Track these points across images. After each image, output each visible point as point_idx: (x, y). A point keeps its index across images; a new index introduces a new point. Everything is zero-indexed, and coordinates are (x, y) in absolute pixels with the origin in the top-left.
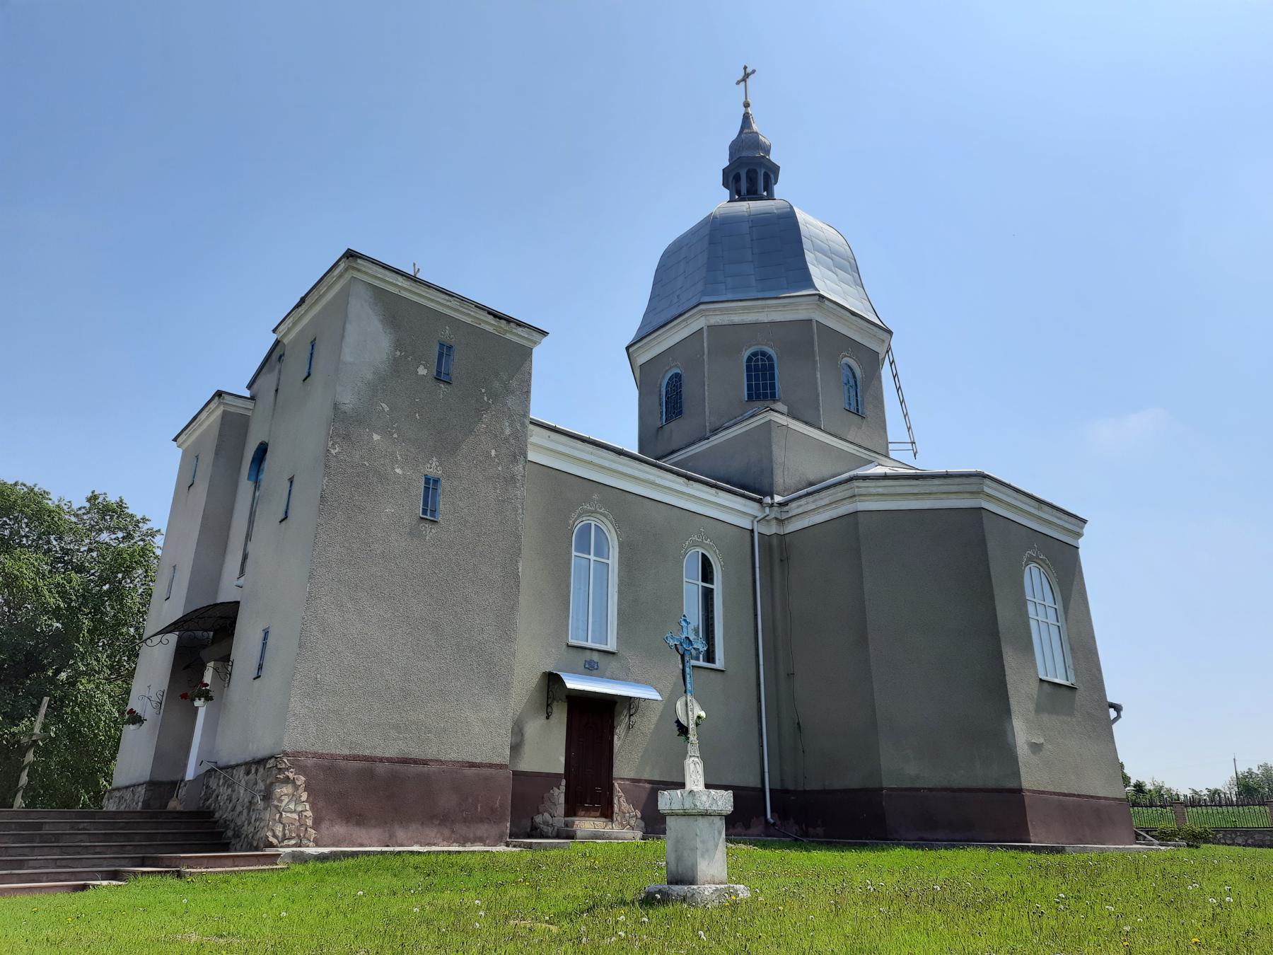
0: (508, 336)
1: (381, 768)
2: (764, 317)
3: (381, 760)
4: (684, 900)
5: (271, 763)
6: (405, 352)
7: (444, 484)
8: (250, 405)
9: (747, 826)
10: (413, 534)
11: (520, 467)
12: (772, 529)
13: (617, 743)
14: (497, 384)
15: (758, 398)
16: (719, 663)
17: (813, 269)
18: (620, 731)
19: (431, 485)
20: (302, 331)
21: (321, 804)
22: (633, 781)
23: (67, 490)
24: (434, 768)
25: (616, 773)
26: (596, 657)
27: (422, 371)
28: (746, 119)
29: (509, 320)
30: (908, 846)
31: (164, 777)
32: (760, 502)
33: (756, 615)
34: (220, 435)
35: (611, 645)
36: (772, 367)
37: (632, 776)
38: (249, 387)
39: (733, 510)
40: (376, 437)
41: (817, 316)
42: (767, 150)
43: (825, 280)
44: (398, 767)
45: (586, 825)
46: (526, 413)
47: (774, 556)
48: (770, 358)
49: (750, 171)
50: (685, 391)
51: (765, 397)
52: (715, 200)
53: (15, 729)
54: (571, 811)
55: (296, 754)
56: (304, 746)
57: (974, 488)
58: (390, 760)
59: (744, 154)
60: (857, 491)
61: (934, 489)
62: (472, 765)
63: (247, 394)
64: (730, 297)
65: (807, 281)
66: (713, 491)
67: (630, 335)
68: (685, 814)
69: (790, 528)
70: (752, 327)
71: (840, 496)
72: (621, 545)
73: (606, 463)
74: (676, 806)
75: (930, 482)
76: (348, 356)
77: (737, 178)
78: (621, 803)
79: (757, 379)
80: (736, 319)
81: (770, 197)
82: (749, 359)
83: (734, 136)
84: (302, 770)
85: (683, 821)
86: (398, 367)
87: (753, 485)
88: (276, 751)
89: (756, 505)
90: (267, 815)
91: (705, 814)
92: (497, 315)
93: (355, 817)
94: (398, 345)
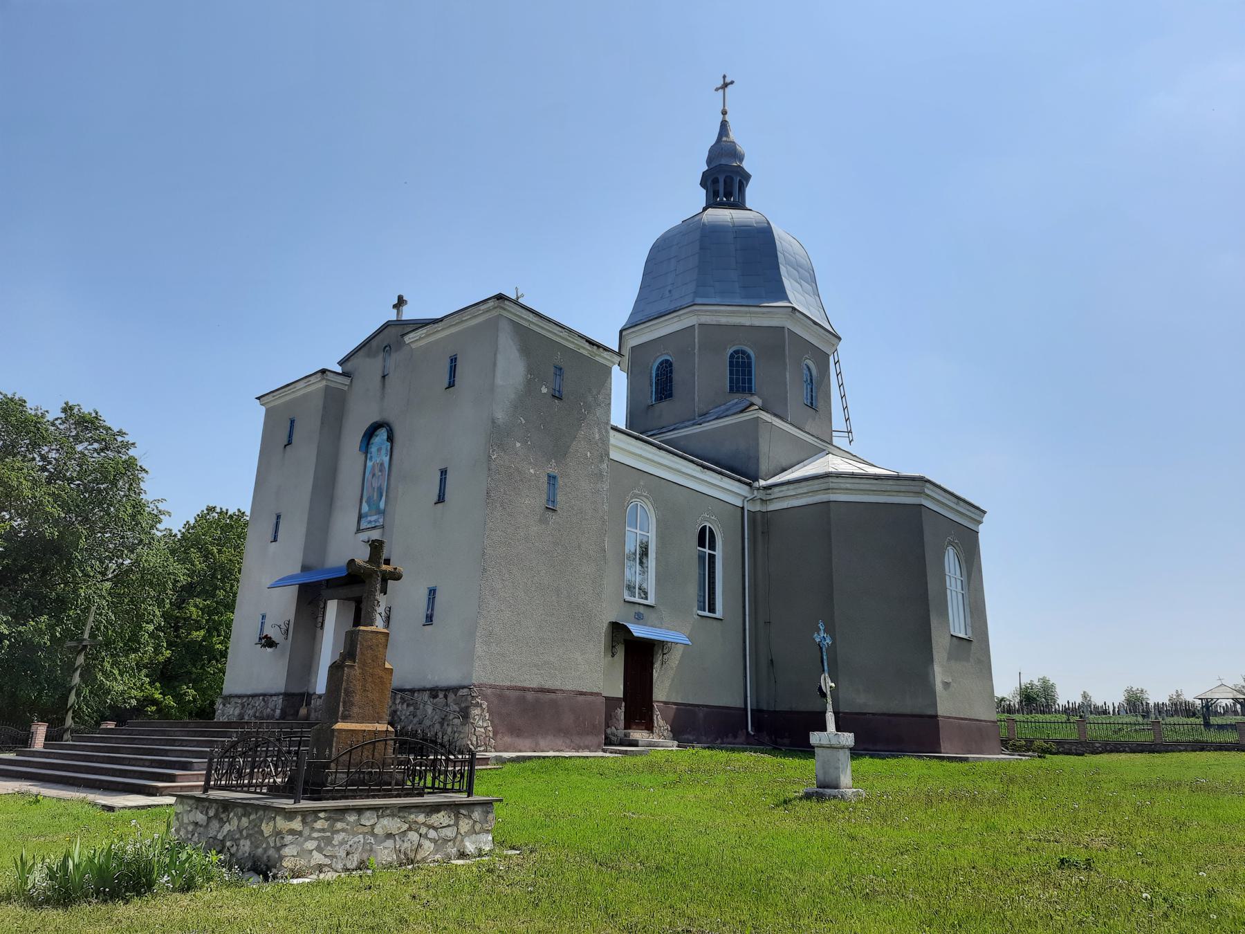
0: (597, 358)
1: (530, 696)
2: (746, 321)
3: (528, 689)
4: (835, 797)
5: (461, 692)
6: (533, 375)
7: (560, 482)
8: (347, 381)
9: (735, 737)
10: (543, 521)
11: (605, 466)
12: (757, 507)
13: (655, 675)
14: (590, 399)
15: (738, 391)
16: (718, 614)
17: (787, 283)
18: (657, 665)
19: (552, 479)
20: (437, 342)
21: (496, 721)
22: (665, 703)
23: (45, 400)
24: (559, 695)
25: (655, 698)
26: (642, 610)
27: (544, 390)
28: (724, 126)
29: (599, 346)
30: (872, 756)
31: (295, 690)
32: (749, 485)
33: (744, 576)
34: (324, 407)
35: (651, 601)
36: (750, 364)
37: (664, 699)
38: (341, 363)
39: (729, 490)
40: (518, 445)
41: (789, 325)
42: (741, 158)
43: (797, 296)
44: (540, 695)
45: (637, 735)
46: (608, 422)
47: (760, 528)
48: (749, 357)
49: (725, 179)
50: (677, 377)
51: (744, 390)
52: (691, 200)
53: (22, 629)
54: (627, 726)
55: (480, 686)
56: (484, 680)
57: (917, 489)
58: (533, 690)
59: (723, 162)
60: (831, 485)
61: (889, 488)
62: (581, 693)
63: (339, 369)
64: (718, 300)
65: (786, 298)
66: (720, 477)
67: (623, 321)
68: (831, 747)
69: (773, 507)
70: (728, 328)
71: (816, 487)
72: (657, 521)
73: (650, 456)
74: (825, 742)
75: (885, 482)
76: (499, 381)
77: (716, 181)
78: (659, 720)
79: (744, 380)
80: (723, 320)
81: (740, 205)
82: (732, 356)
83: (713, 140)
84: (485, 698)
85: (828, 751)
86: (530, 385)
87: (742, 469)
88: (465, 683)
89: (747, 488)
90: (466, 728)
91: (843, 748)
92: (591, 342)
93: (516, 731)
94: (530, 370)
